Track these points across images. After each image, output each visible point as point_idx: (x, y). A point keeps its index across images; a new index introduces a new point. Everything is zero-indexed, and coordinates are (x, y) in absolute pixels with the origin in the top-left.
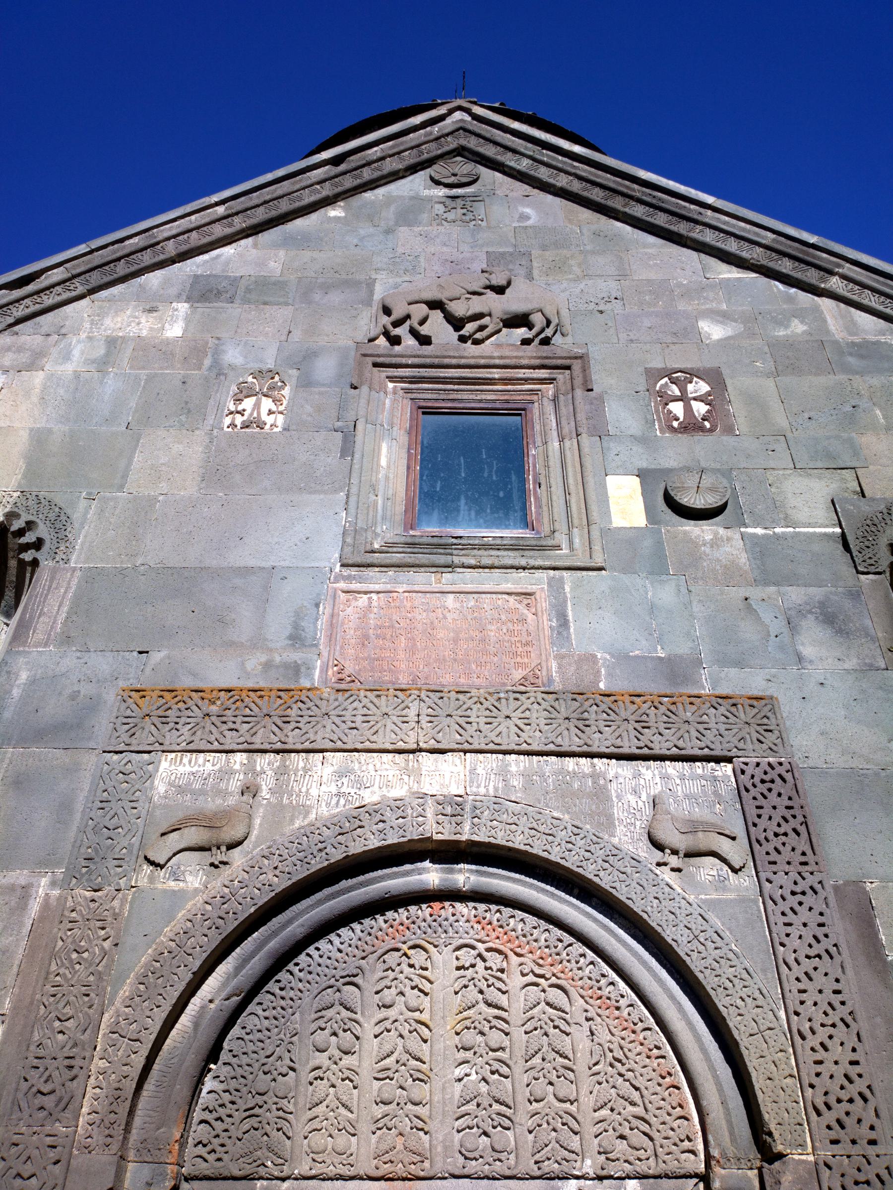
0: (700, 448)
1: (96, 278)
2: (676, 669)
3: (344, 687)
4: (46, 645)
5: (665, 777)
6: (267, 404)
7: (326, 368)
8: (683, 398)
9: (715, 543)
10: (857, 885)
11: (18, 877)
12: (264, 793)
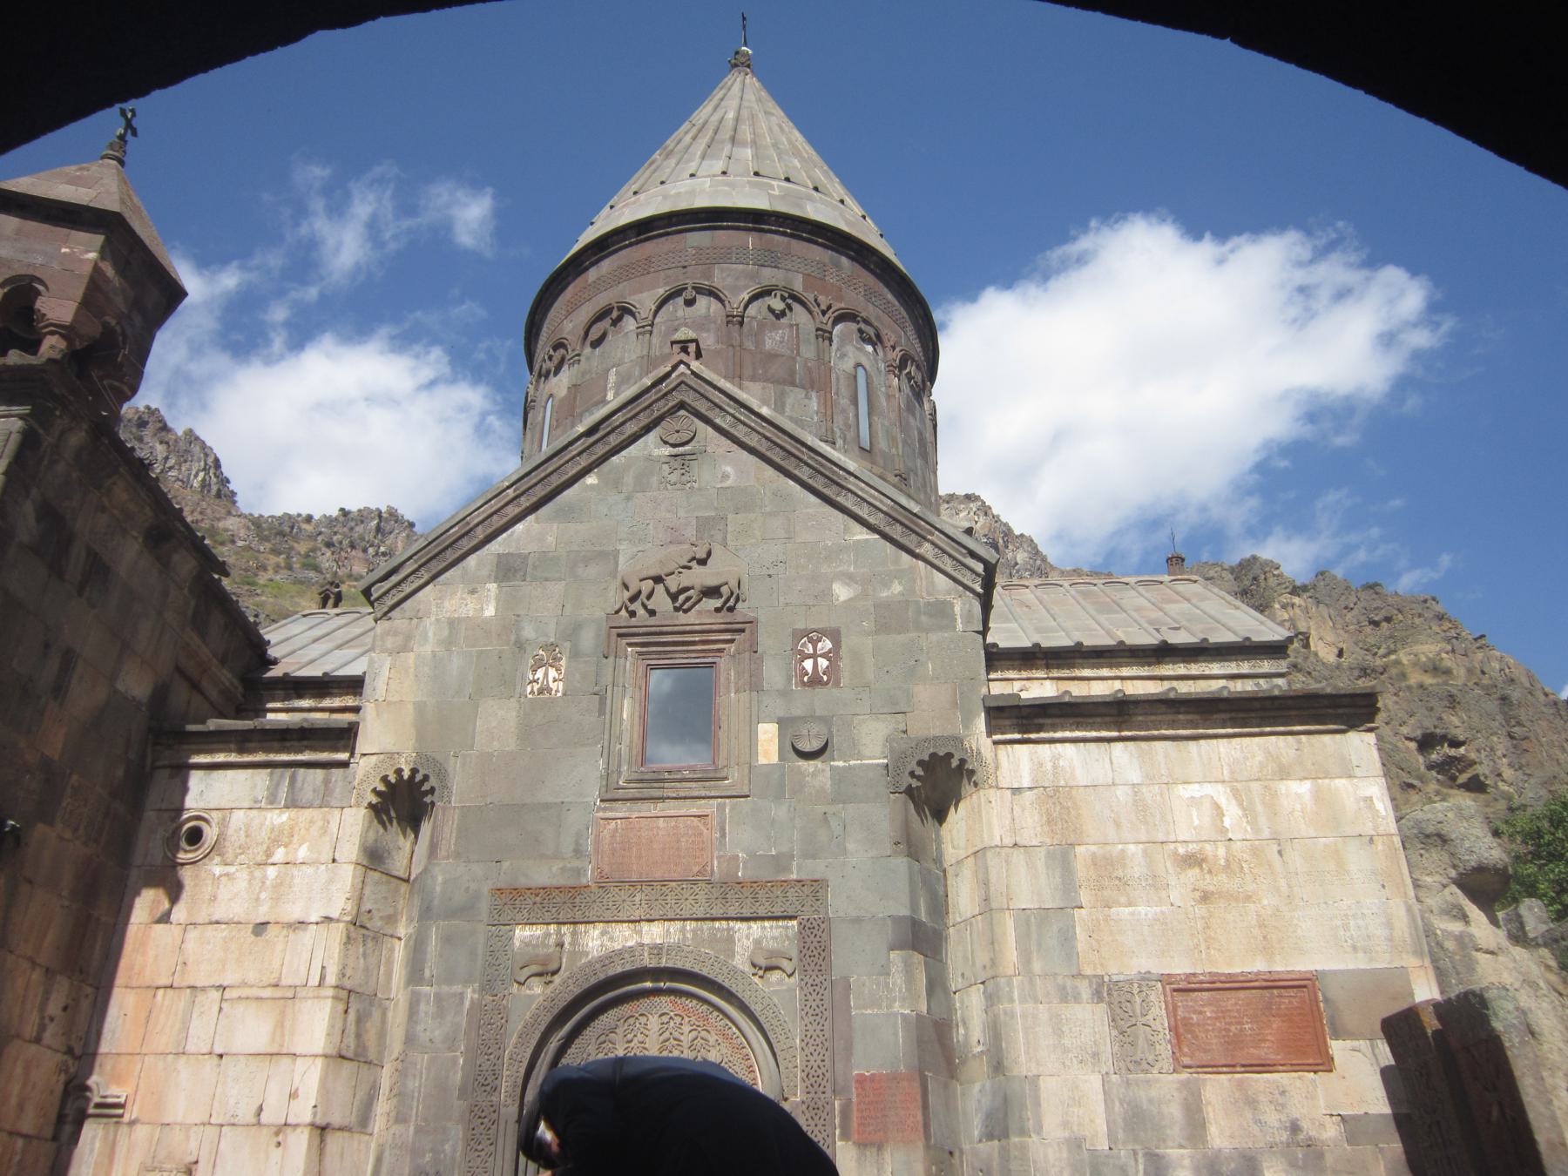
0: (820, 700)
1: (436, 566)
2: (781, 862)
3: (603, 883)
4: (447, 858)
5: (764, 928)
6: (552, 673)
7: (588, 639)
8: (814, 656)
9: (814, 775)
10: (846, 980)
11: (457, 988)
12: (567, 946)
